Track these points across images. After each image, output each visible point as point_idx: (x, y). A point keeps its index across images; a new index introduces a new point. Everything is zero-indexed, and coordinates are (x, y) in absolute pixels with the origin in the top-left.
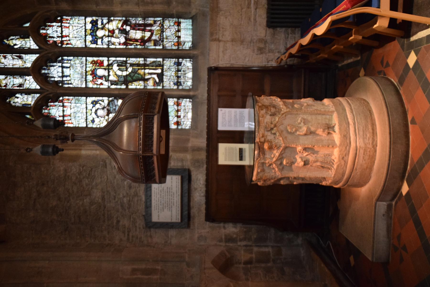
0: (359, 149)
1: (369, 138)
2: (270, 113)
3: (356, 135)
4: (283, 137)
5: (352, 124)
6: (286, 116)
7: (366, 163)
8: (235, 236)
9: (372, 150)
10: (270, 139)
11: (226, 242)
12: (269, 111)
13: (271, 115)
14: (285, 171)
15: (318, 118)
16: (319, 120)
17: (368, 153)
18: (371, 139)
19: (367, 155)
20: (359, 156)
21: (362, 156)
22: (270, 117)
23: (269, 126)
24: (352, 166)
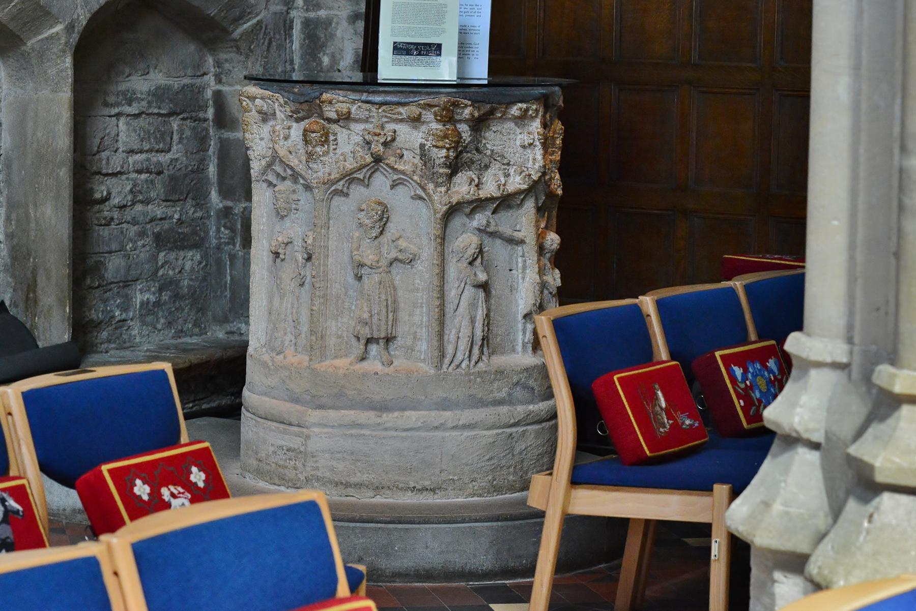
0: (303, 433)
1: (332, 469)
2: (429, 144)
3: (340, 426)
4: (341, 183)
5: (379, 420)
6: (421, 198)
7: (268, 456)
8: (326, 60)
9: (300, 476)
10: (336, 140)
11: (307, 23)
12: (434, 143)
13: (422, 146)
14: (267, 194)
15: (418, 311)
16: (411, 315)
17: (292, 463)
18: (328, 474)
19: (286, 460)
20: (285, 432)
21: (284, 443)
22: (418, 145)
23: (376, 138)
24: (261, 412)
